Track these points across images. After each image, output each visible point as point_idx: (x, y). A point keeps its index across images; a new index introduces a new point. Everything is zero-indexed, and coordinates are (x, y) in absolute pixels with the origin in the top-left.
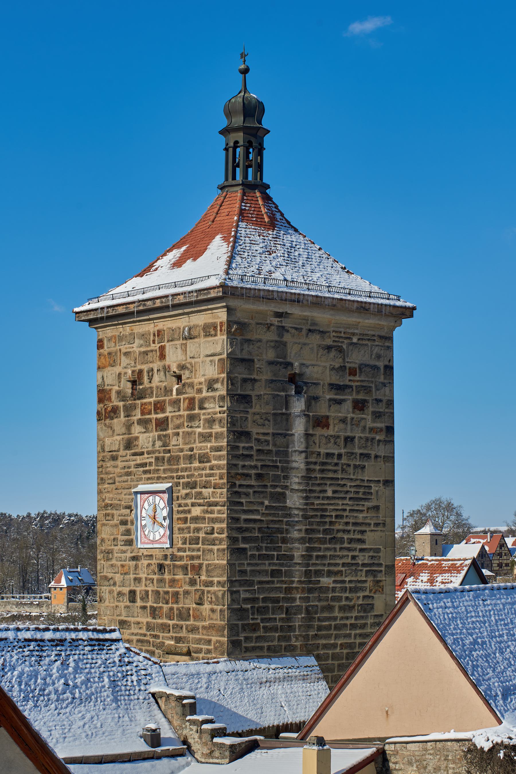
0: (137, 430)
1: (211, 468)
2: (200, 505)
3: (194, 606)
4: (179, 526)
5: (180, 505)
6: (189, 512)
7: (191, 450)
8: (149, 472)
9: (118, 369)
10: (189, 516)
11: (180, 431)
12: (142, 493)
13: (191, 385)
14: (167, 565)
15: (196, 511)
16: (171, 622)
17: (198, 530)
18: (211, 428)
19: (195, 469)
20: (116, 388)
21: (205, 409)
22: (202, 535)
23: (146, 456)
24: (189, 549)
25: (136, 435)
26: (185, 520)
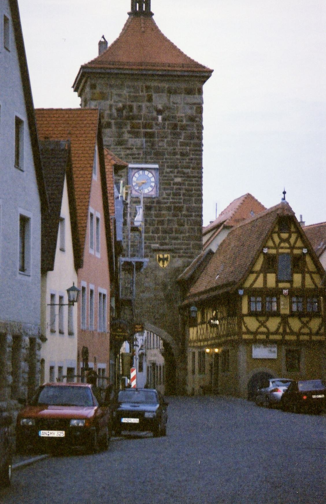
0: (126, 136)
1: (189, 159)
2: (181, 177)
3: (176, 226)
4: (163, 187)
5: (166, 176)
6: (173, 180)
7: (174, 149)
8: (138, 158)
9: (109, 102)
10: (172, 182)
11: (166, 140)
12: (133, 168)
13: (174, 117)
14: (154, 206)
15: (178, 180)
16: (156, 235)
17: (180, 189)
18: (191, 140)
19: (177, 159)
20: (108, 112)
21: (186, 130)
22: (182, 192)
23: (135, 150)
24: (173, 199)
25: (126, 138)
26: (170, 184)
